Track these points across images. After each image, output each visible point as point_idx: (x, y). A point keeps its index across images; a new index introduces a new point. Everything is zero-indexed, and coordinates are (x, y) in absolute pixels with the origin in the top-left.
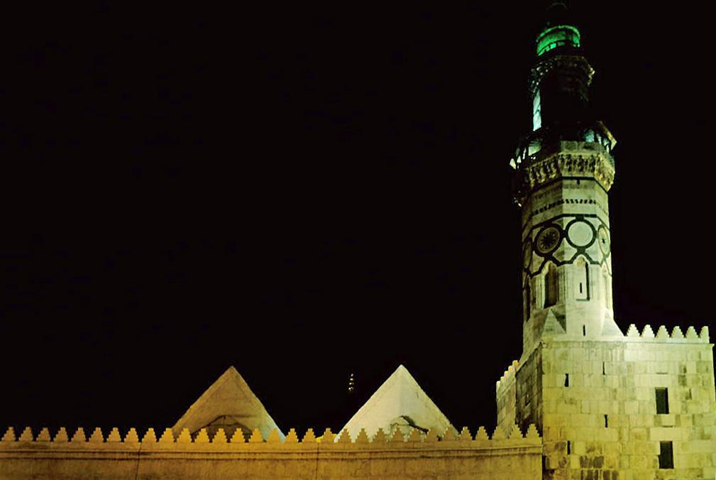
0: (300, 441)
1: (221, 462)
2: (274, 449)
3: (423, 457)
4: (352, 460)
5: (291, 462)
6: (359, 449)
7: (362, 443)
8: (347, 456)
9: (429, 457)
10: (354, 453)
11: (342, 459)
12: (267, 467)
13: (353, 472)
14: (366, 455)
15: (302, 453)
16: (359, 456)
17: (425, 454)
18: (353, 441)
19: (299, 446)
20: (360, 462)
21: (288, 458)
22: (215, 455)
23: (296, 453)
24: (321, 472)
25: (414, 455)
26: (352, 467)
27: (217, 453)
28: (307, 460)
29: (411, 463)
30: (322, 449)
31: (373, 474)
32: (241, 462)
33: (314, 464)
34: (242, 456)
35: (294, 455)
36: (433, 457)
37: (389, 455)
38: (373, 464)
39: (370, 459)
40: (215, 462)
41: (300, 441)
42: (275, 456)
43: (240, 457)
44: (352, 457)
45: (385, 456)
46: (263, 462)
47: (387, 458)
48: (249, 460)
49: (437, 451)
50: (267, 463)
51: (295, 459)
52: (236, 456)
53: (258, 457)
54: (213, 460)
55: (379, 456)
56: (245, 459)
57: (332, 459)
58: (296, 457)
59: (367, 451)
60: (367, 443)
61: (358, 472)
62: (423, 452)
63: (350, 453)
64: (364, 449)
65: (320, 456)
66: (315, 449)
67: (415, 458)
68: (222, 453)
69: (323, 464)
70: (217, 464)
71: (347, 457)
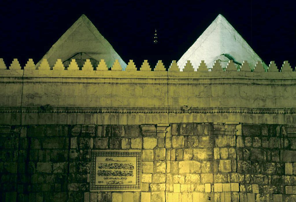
0: (152, 70)
1: (91, 84)
2: (132, 75)
3: (254, 84)
4: (196, 85)
5: (146, 85)
6: (201, 76)
7: (202, 72)
8: (191, 82)
9: (258, 84)
10: (197, 79)
11: (188, 84)
12: (127, 90)
13: (198, 94)
14: (207, 82)
15: (155, 79)
16: (201, 81)
17: (255, 82)
18: (196, 70)
19: (152, 74)
20: (202, 87)
21: (144, 82)
22: (85, 79)
23: (150, 79)
24: (171, 93)
25: (245, 82)
26: (197, 90)
27: (86, 78)
28: (159, 84)
29: (245, 88)
30: (171, 76)
31: (213, 96)
32: (106, 85)
33: (165, 88)
34: (107, 81)
35: (149, 80)
36: (262, 84)
37: (226, 81)
38: (213, 88)
39: (210, 84)
40: (85, 85)
41: (152, 70)
42: (133, 81)
43: (106, 82)
44: (195, 82)
45: (222, 82)
46: (124, 85)
47: (224, 84)
48: (113, 83)
49: (265, 79)
50: (127, 86)
51: (150, 84)
52: (103, 81)
53: (119, 81)
54: (84, 83)
55: (217, 82)
56: (109, 83)
57: (180, 84)
58: (150, 81)
59: (207, 78)
60: (207, 72)
61: (202, 93)
62: (254, 79)
63: (194, 79)
64: (205, 76)
65: (170, 82)
66: (165, 76)
67: (247, 84)
68: (91, 78)
69: (172, 88)
70: (87, 86)
71: (192, 82)
